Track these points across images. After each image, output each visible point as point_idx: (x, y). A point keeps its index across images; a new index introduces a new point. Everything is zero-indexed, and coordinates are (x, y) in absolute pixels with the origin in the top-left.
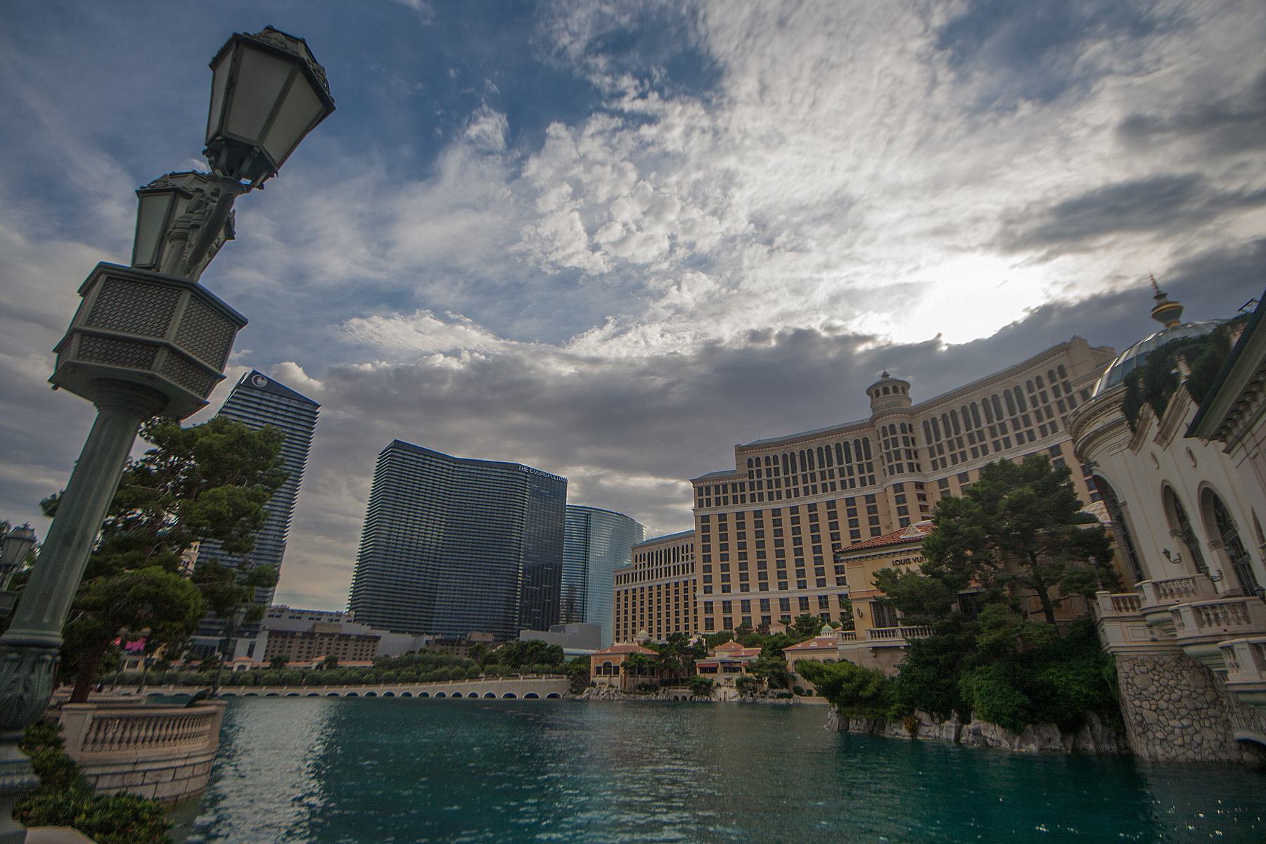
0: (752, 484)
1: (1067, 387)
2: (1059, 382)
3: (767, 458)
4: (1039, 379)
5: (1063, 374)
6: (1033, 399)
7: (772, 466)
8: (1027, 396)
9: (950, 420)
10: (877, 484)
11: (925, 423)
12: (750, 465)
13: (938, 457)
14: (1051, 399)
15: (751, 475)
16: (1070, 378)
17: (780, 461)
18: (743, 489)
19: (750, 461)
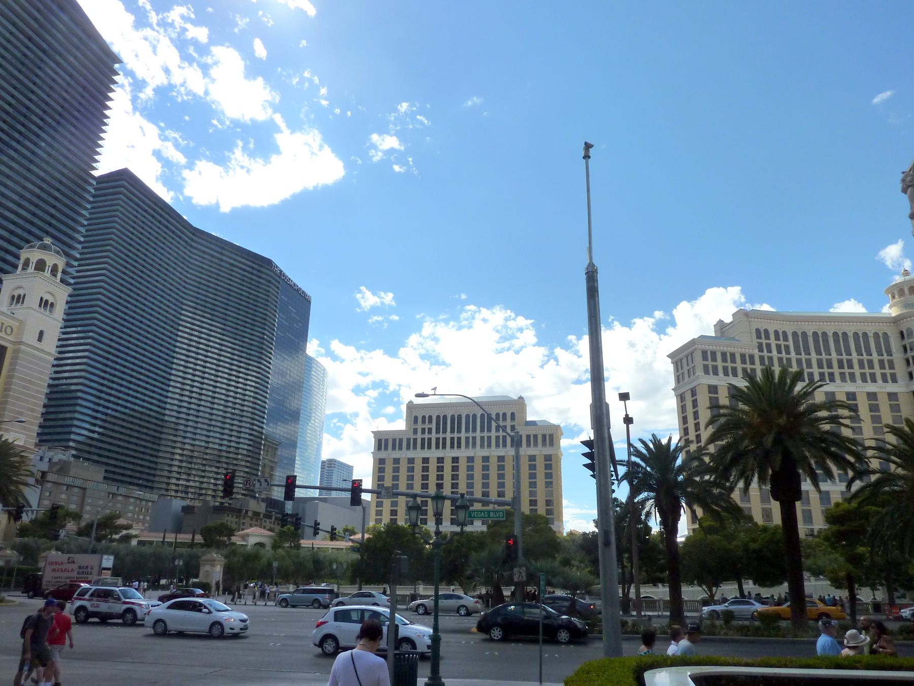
3: (776, 332)
7: (782, 343)
12: (759, 337)
17: (790, 338)
19: (758, 331)
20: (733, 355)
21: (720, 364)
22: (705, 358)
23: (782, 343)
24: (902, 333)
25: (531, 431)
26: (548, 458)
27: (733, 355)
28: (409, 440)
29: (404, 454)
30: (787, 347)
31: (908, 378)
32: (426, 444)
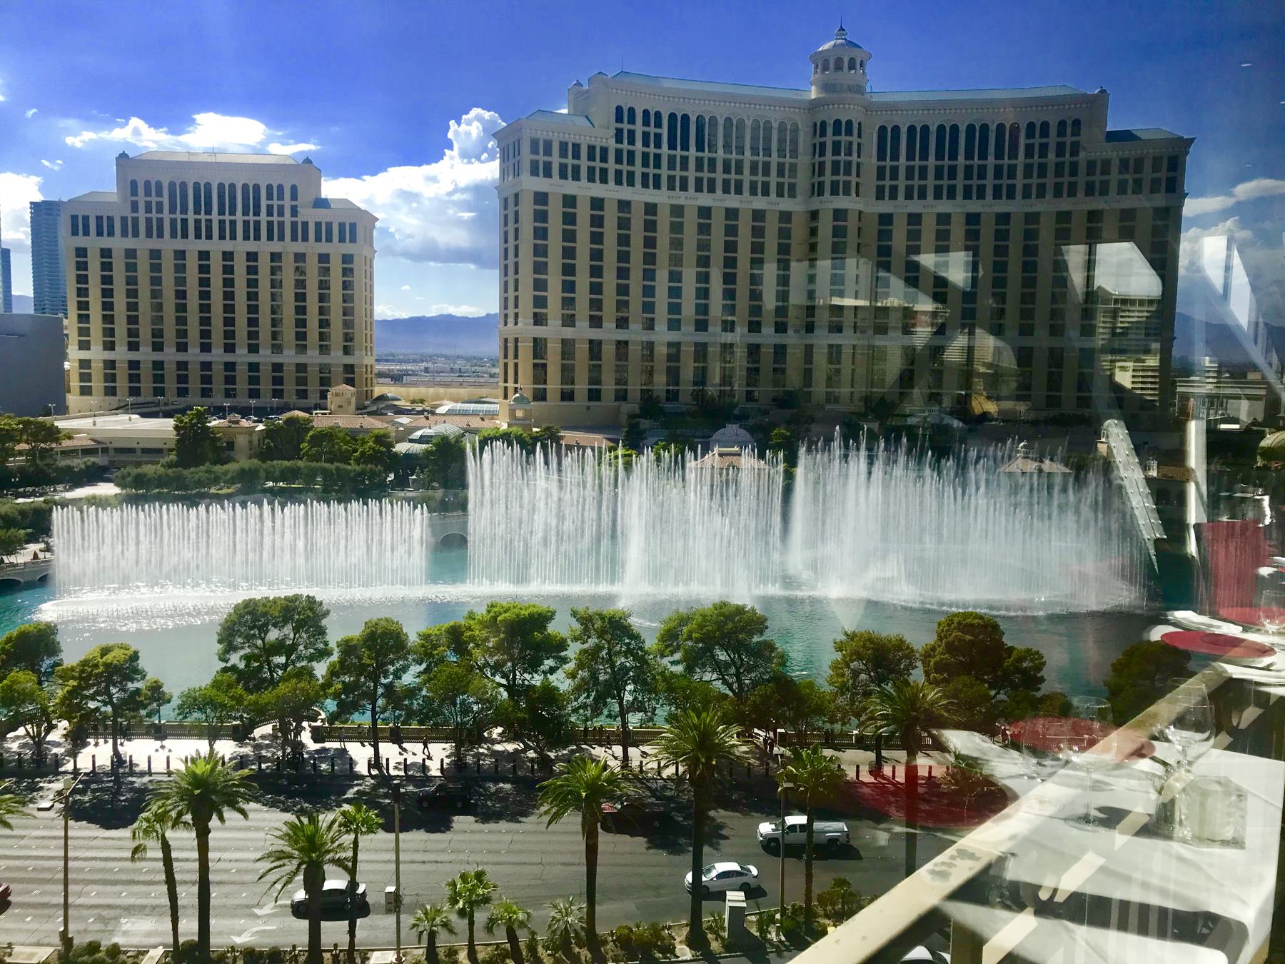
0: (619, 153)
1: (1075, 153)
2: (1069, 139)
3: (646, 113)
4: (1045, 125)
5: (1076, 133)
6: (1029, 151)
8: (1022, 141)
9: (918, 136)
10: (799, 198)
11: (882, 129)
12: (619, 119)
13: (887, 183)
14: (1051, 156)
15: (619, 136)
16: (1083, 138)
18: (604, 159)
19: (619, 110)
20: (576, 147)
21: (556, 160)
22: (534, 150)
23: (652, 130)
24: (815, 125)
25: (322, 215)
26: (347, 259)
27: (576, 147)
28: (124, 220)
29: (118, 244)
30: (658, 137)
31: (809, 193)
32: (155, 230)
